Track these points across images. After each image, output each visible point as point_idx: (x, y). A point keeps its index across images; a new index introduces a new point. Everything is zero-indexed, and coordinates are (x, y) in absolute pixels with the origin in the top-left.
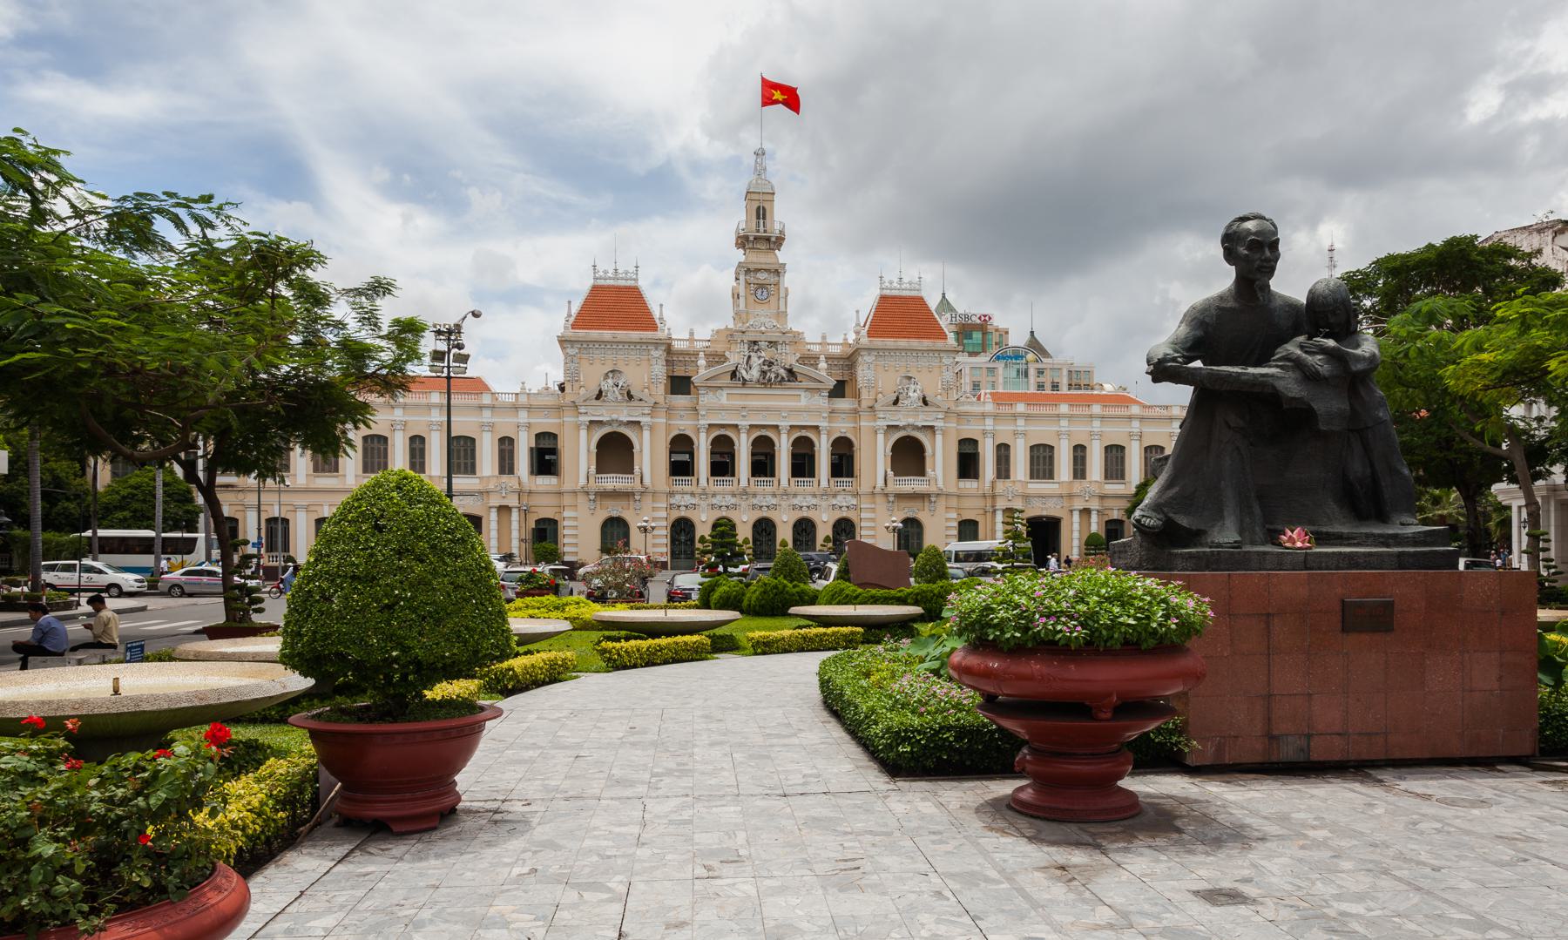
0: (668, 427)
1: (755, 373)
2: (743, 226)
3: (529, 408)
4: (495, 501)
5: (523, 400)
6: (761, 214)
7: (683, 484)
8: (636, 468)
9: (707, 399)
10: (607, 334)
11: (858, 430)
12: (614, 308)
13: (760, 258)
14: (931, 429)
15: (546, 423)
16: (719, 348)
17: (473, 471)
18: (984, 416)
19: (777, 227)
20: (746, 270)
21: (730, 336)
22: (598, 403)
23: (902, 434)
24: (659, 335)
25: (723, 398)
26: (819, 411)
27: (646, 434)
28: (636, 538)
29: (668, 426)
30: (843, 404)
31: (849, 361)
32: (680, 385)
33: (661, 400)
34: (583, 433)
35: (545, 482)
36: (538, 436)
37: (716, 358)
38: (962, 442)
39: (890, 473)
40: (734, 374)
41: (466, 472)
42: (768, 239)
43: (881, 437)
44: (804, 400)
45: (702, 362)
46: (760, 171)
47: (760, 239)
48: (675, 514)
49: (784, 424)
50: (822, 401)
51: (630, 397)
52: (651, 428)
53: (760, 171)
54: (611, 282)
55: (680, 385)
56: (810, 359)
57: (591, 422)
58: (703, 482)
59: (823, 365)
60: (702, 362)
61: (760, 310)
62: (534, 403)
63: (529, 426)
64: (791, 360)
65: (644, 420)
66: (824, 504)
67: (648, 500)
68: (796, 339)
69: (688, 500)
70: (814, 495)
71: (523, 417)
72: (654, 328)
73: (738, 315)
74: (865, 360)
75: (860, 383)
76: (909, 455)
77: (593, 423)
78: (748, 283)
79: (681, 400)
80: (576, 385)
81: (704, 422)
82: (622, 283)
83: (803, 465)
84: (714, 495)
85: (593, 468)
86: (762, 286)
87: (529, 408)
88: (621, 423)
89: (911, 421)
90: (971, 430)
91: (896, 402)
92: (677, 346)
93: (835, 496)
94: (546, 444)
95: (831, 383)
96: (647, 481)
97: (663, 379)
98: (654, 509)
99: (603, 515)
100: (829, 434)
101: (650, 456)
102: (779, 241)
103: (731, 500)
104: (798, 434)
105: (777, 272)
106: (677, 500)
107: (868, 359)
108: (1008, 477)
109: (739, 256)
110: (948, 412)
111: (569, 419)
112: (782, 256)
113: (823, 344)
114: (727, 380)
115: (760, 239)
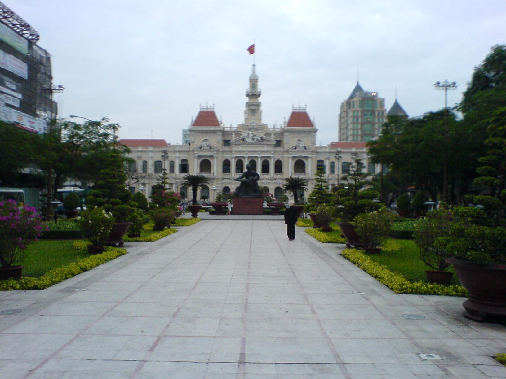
2: (248, 90)
3: (179, 152)
5: (177, 149)
7: (227, 175)
8: (212, 171)
9: (235, 148)
11: (283, 157)
12: (206, 119)
13: (253, 101)
14: (306, 157)
15: (184, 156)
16: (240, 130)
18: (326, 152)
19: (258, 90)
20: (248, 105)
21: (242, 127)
23: (298, 159)
25: (240, 148)
26: (270, 152)
27: (215, 159)
28: (211, 193)
30: (279, 149)
31: (282, 133)
32: (227, 143)
34: (196, 160)
37: (238, 133)
38: (319, 161)
39: (293, 172)
40: (243, 140)
43: (290, 160)
44: (266, 148)
45: (234, 136)
46: (254, 71)
47: (254, 94)
48: (224, 186)
49: (259, 156)
50: (272, 149)
51: (211, 148)
52: (217, 157)
53: (254, 71)
54: (205, 110)
56: (268, 134)
57: (199, 156)
58: (233, 175)
59: (272, 136)
60: (234, 136)
62: (181, 150)
63: (179, 157)
64: (262, 135)
66: (272, 182)
67: (215, 181)
68: (264, 127)
69: (228, 181)
70: (269, 179)
71: (177, 155)
73: (246, 119)
75: (285, 141)
76: (300, 165)
77: (199, 157)
79: (227, 149)
81: (234, 156)
82: (209, 110)
83: (266, 169)
85: (199, 171)
87: (179, 152)
88: (208, 156)
89: (300, 154)
90: (321, 157)
91: (295, 148)
92: (227, 130)
93: (275, 179)
94: (184, 163)
95: (275, 142)
96: (215, 175)
98: (217, 184)
100: (274, 158)
101: (216, 167)
102: (259, 95)
105: (258, 105)
107: (286, 134)
108: (333, 173)
109: (247, 100)
110: (313, 152)
111: (191, 155)
112: (260, 99)
113: (274, 128)
114: (241, 142)
115: (254, 94)
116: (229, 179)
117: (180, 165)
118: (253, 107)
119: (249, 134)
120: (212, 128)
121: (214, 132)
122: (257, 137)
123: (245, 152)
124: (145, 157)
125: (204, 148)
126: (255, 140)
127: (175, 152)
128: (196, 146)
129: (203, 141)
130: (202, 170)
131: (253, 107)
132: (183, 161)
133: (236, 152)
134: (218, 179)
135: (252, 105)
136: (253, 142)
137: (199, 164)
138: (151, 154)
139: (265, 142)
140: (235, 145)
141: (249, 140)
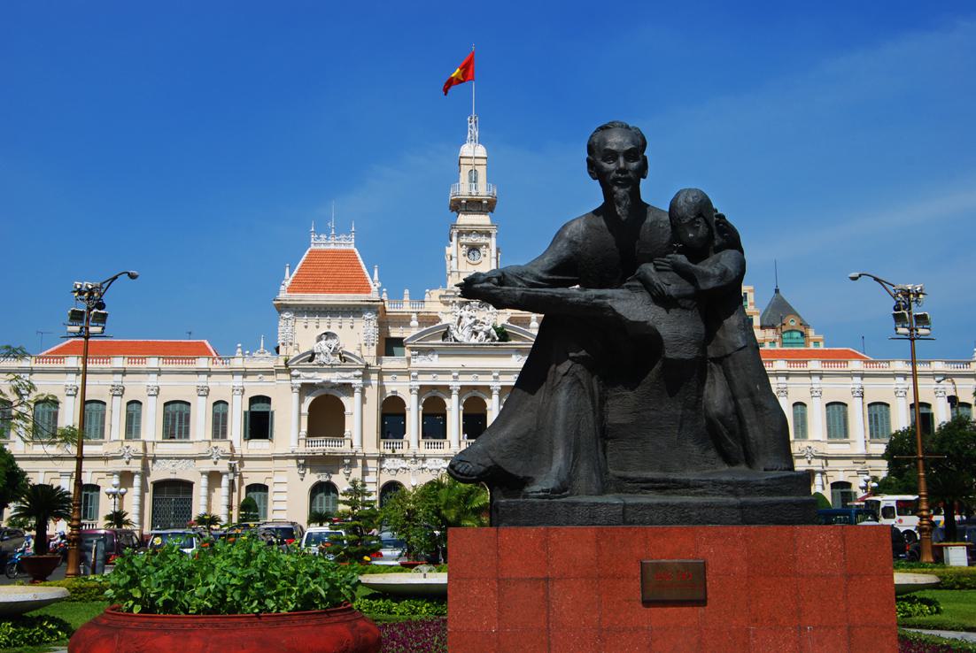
1: (467, 332)
3: (245, 373)
4: (208, 466)
8: (347, 429)
15: (256, 387)
17: (187, 434)
22: (307, 365)
25: (435, 362)
29: (381, 388)
33: (372, 361)
35: (258, 447)
36: (253, 400)
40: (445, 336)
41: (180, 437)
42: (480, 202)
45: (414, 323)
48: (386, 478)
49: (496, 385)
60: (414, 323)
65: (358, 383)
69: (399, 463)
72: (368, 290)
77: (306, 389)
80: (291, 348)
82: (338, 248)
84: (424, 459)
85: (304, 428)
88: (334, 386)
94: (259, 407)
96: (356, 443)
97: (375, 339)
99: (312, 478)
101: (360, 418)
106: (388, 463)
116: (402, 457)
117: (245, 413)
119: (461, 317)
121: (355, 311)
122: (486, 328)
124: (136, 387)
125: (322, 358)
126: (481, 334)
128: (296, 354)
129: (319, 339)
130: (313, 432)
132: (254, 400)
134: (365, 459)
135: (469, 233)
136: (476, 341)
137: (305, 409)
138: (153, 380)
141: (463, 335)
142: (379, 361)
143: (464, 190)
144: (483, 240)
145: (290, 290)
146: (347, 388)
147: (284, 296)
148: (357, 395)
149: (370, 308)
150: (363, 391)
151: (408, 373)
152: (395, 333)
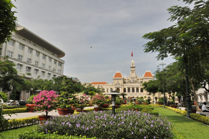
0: (123, 87)
3: (110, 86)
6: (133, 64)
10: (117, 78)
15: (111, 87)
24: (122, 78)
25: (129, 84)
32: (125, 83)
33: (122, 84)
36: (111, 88)
40: (130, 82)
44: (137, 84)
49: (135, 87)
52: (122, 87)
55: (125, 83)
61: (133, 74)
63: (110, 88)
64: (136, 80)
72: (122, 77)
74: (144, 79)
77: (116, 87)
78: (131, 72)
79: (125, 84)
86: (133, 72)
87: (110, 86)
103: (130, 95)
104: (137, 88)
111: (114, 87)
118: (133, 71)
120: (120, 78)
121: (121, 79)
123: (131, 85)
127: (109, 86)
131: (133, 71)
133: (128, 85)
139: (137, 82)
140: (128, 83)
142: (123, 84)
143: (132, 66)
144: (134, 71)
145: (114, 77)
146: (120, 87)
147: (113, 78)
148: (121, 88)
149: (122, 79)
150: (122, 87)
151: (126, 85)
152: (125, 81)
